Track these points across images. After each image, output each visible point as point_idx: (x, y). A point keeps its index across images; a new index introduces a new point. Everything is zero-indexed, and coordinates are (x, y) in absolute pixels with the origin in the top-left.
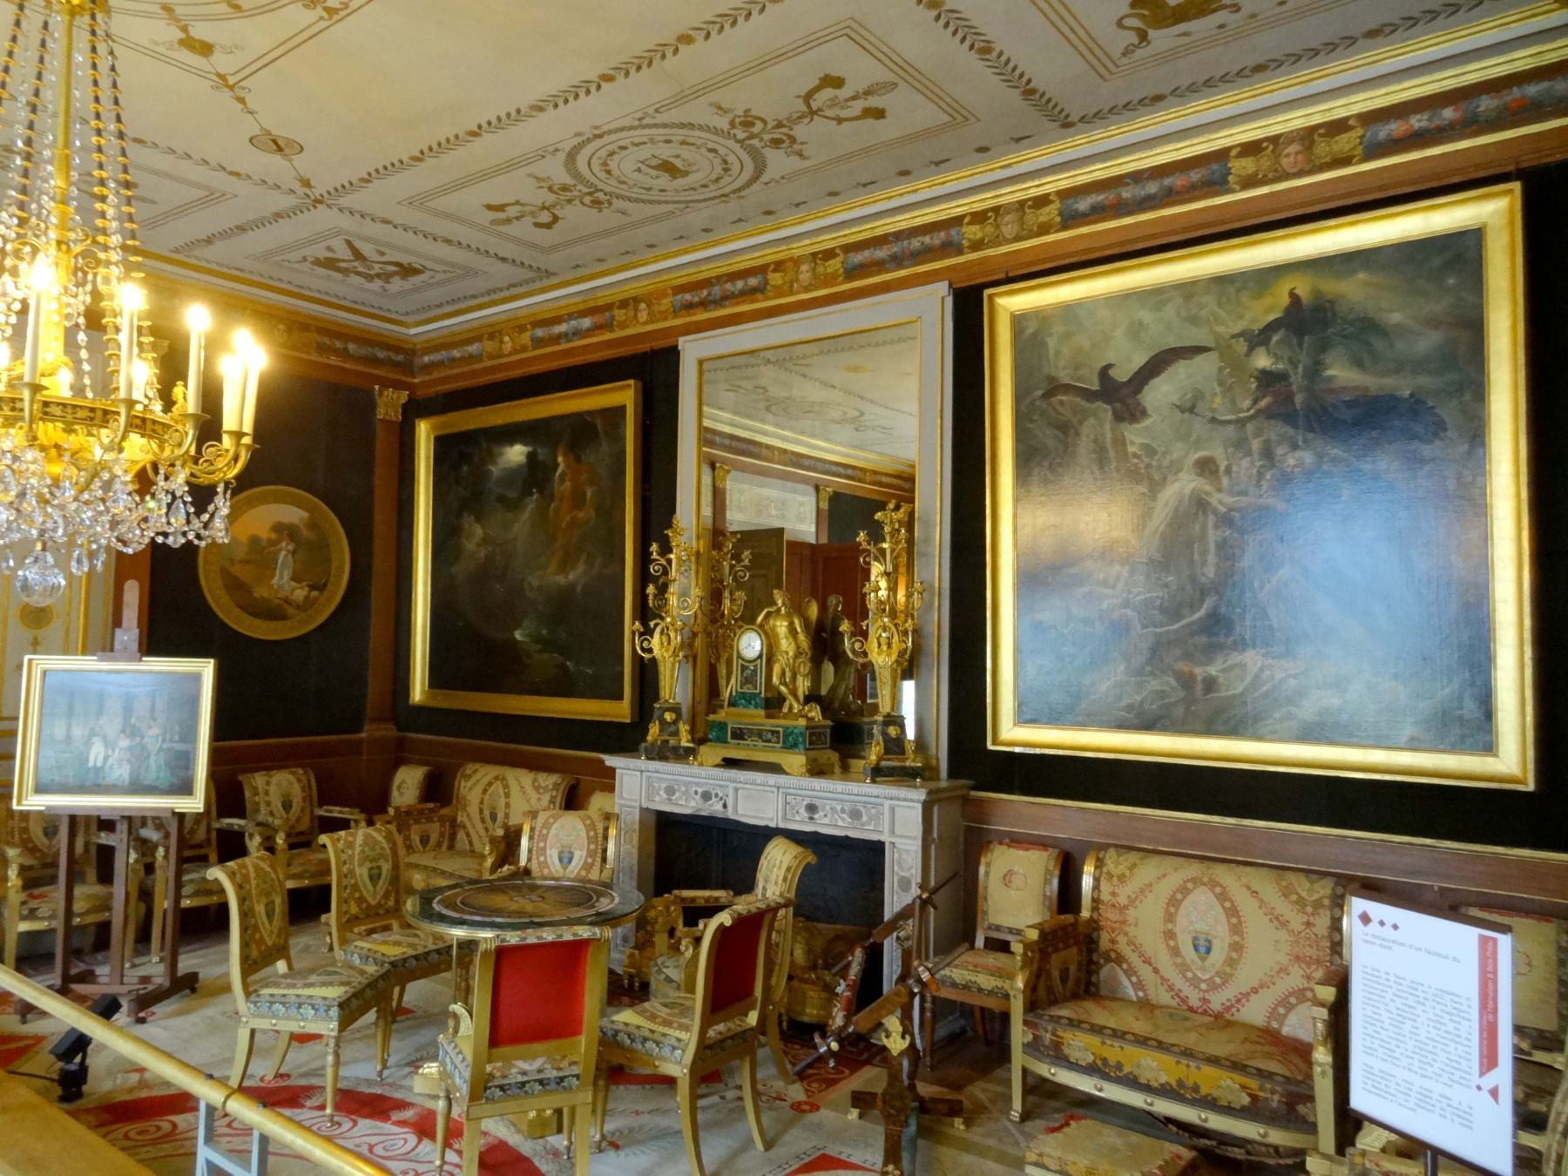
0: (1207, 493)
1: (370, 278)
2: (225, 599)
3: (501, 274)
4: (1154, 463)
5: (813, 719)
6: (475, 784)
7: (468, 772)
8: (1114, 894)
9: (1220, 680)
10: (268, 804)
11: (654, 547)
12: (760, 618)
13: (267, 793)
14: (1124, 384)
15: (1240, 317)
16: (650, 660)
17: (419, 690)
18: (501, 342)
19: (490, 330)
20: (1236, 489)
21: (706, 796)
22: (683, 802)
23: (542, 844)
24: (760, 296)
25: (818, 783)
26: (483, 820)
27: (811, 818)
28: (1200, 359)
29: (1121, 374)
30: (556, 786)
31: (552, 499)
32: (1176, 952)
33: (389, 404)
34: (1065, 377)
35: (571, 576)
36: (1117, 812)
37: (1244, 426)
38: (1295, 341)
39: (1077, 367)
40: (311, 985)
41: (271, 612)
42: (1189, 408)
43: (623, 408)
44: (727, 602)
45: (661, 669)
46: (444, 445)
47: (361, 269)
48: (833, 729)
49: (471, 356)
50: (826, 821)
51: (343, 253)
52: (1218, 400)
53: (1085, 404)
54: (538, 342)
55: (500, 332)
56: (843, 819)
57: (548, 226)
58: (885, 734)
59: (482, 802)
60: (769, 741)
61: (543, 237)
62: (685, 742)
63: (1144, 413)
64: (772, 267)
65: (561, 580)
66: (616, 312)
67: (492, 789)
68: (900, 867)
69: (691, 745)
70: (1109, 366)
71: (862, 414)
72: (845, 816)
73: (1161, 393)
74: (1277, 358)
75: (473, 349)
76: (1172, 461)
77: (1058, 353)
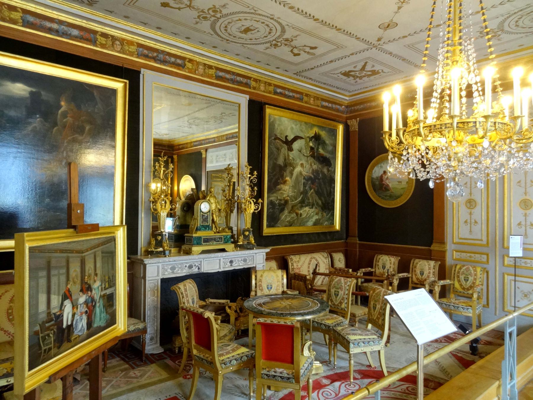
22: (179, 272)
24: (181, 68)
28: (302, 140)
50: (236, 265)
53: (282, 144)
60: (219, 241)
73: (296, 145)
77: (277, 129)
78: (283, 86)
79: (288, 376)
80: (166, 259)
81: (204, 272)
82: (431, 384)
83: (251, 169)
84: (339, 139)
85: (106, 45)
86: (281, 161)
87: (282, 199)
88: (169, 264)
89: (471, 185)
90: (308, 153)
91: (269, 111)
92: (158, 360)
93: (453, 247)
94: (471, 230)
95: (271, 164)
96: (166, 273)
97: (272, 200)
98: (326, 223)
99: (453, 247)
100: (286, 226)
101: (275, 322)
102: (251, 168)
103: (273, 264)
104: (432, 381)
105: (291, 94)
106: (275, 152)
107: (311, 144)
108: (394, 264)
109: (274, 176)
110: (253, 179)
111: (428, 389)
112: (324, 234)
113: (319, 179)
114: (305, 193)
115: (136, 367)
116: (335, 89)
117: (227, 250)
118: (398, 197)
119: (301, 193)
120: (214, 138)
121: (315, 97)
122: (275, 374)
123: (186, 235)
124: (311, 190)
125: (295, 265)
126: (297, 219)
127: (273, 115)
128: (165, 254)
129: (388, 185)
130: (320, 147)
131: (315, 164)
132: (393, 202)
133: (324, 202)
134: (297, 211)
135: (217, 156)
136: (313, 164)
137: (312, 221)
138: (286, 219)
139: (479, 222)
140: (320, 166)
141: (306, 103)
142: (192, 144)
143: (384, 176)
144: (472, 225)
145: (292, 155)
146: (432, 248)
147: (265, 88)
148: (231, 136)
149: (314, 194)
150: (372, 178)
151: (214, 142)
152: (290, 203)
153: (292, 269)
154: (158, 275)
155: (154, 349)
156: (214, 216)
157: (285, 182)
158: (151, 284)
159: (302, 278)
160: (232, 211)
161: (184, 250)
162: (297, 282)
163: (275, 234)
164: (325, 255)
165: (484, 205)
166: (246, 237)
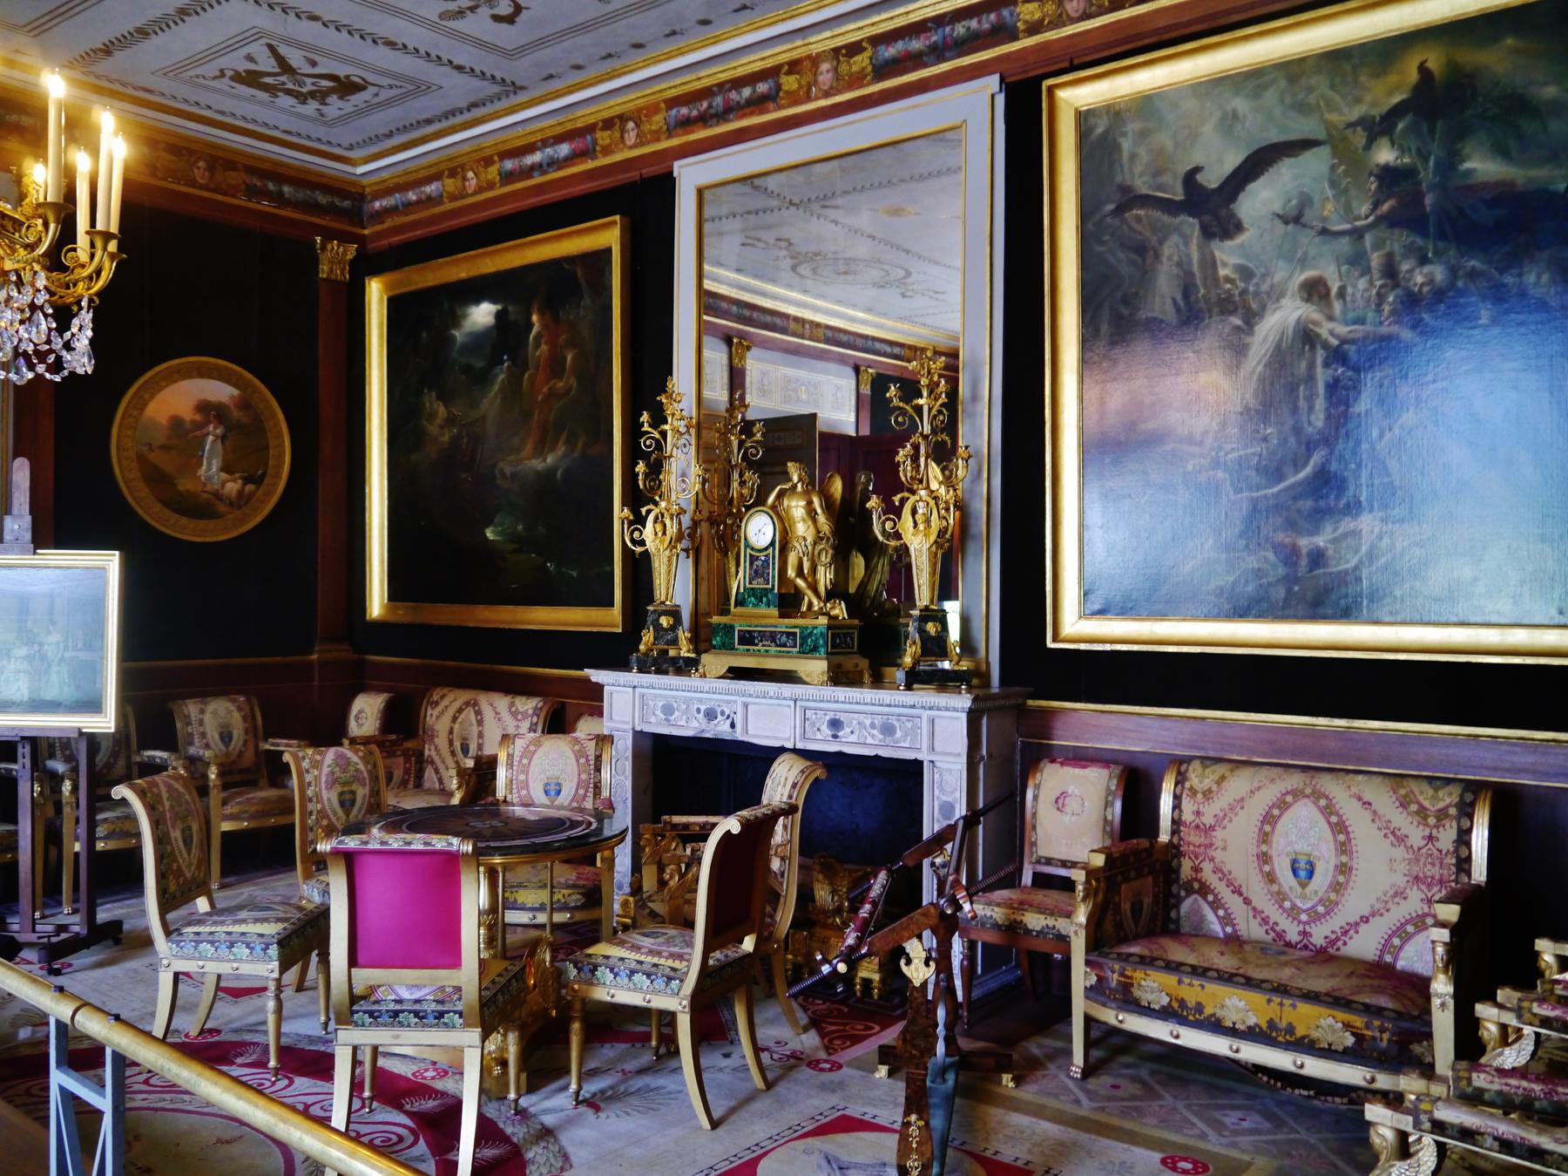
0: (1316, 323)
1: (302, 98)
2: (144, 492)
3: (459, 89)
4: (1251, 289)
5: (836, 617)
6: (442, 713)
7: (435, 698)
8: (1198, 813)
9: (1330, 552)
10: (203, 735)
11: (645, 417)
12: (771, 499)
13: (201, 723)
14: (1214, 191)
15: (1358, 100)
16: (641, 554)
17: (377, 602)
18: (465, 179)
19: (451, 165)
20: (1351, 315)
21: (711, 715)
22: (683, 723)
23: (522, 777)
24: (771, 106)
25: (842, 692)
26: (453, 753)
27: (835, 736)
29: (1212, 179)
30: (537, 711)
31: (526, 368)
32: (1271, 878)
33: (333, 259)
34: (1142, 186)
35: (550, 460)
36: (1203, 719)
37: (1361, 237)
38: (1425, 128)
39: (1158, 173)
40: (243, 921)
41: (201, 508)
42: (1294, 219)
43: (608, 251)
44: (735, 485)
45: (656, 564)
46: (397, 307)
47: (290, 86)
48: (861, 630)
49: (429, 198)
50: (853, 738)
51: (267, 64)
52: (1330, 206)
53: (1166, 218)
54: (508, 177)
55: (463, 167)
56: (873, 736)
57: (510, 19)
58: (922, 631)
59: (451, 732)
60: (785, 646)
61: (507, 36)
62: (685, 651)
63: (1239, 227)
64: (786, 68)
65: (537, 464)
66: (599, 134)
67: (462, 716)
68: (942, 790)
69: (693, 655)
70: (1197, 170)
71: (908, 274)
72: (875, 732)
74: (1403, 151)
75: (431, 189)
76: (1272, 286)
77: (1133, 157)
85: (610, 145)
88: (660, 696)
106: (1126, 270)
145: (1228, 255)
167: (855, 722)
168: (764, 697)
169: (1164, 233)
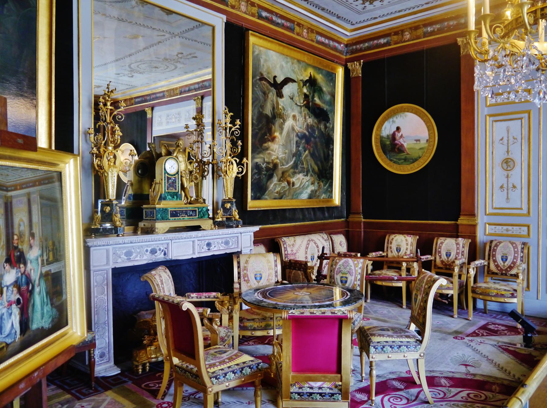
15: (302, 75)
20: (300, 126)
22: (138, 258)
28: (295, 84)
50: (215, 249)
52: (297, 98)
53: (269, 87)
56: (222, 246)
60: (191, 216)
73: (287, 90)
77: (263, 65)
78: (270, 8)
79: (331, 392)
80: (120, 239)
81: (173, 258)
82: (494, 387)
83: (231, 117)
84: (338, 86)
86: (268, 111)
87: (271, 161)
89: (508, 141)
90: (300, 101)
91: (253, 40)
92: (114, 385)
93: (486, 219)
94: (508, 197)
95: (256, 113)
96: (119, 260)
97: (257, 163)
98: (324, 196)
99: (486, 219)
100: (275, 199)
101: (318, 314)
102: (231, 115)
103: (261, 249)
104: (494, 384)
105: (279, 21)
106: (261, 97)
107: (305, 90)
108: (412, 245)
109: (260, 129)
110: (235, 131)
111: (494, 394)
112: (321, 209)
113: (315, 138)
114: (297, 155)
115: (82, 397)
116: (334, 19)
117: (203, 227)
118: (415, 160)
119: (294, 155)
120: (163, 92)
121: (309, 28)
122: (311, 391)
123: (144, 206)
124: (305, 151)
125: (289, 250)
126: (289, 189)
127: (258, 45)
128: (116, 232)
129: (402, 145)
130: (316, 95)
131: (310, 117)
132: (409, 167)
133: (321, 168)
134: (289, 179)
135: (168, 116)
136: (307, 117)
137: (306, 192)
138: (275, 189)
139: (519, 187)
140: (316, 121)
141: (298, 34)
142: (133, 101)
143: (397, 133)
144: (510, 191)
146: (459, 222)
147: (247, 9)
148: (187, 89)
149: (309, 158)
150: (382, 137)
151: (163, 97)
152: (280, 167)
153: (285, 254)
154: (108, 263)
155: (106, 369)
156: (184, 179)
157: (273, 139)
158: (98, 277)
159: (302, 266)
160: (203, 177)
161: (142, 228)
162: (294, 271)
163: (262, 209)
164: (325, 236)
165: (525, 165)
166: (226, 210)
167: (216, 242)
168: (182, 239)
169: (270, 91)
